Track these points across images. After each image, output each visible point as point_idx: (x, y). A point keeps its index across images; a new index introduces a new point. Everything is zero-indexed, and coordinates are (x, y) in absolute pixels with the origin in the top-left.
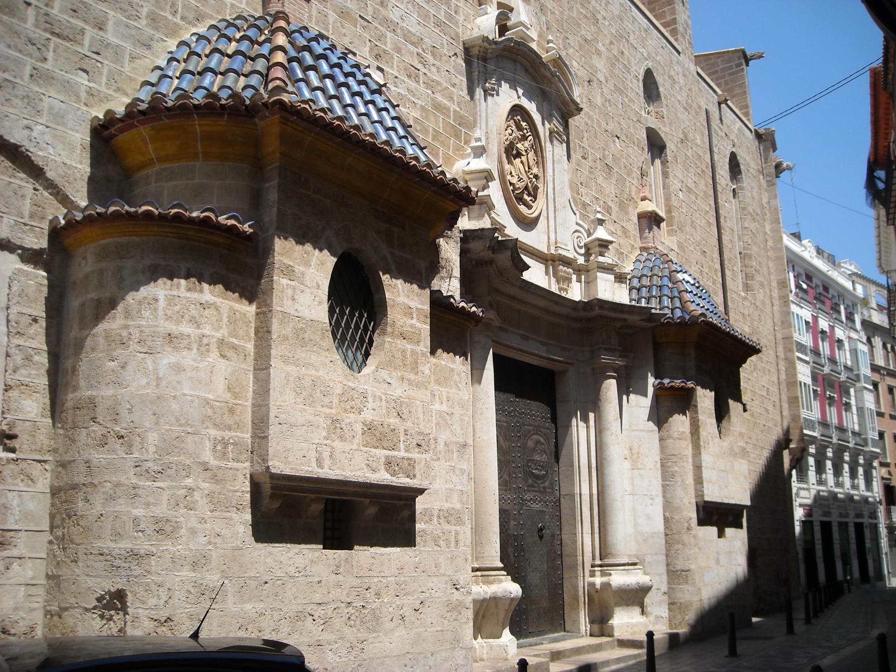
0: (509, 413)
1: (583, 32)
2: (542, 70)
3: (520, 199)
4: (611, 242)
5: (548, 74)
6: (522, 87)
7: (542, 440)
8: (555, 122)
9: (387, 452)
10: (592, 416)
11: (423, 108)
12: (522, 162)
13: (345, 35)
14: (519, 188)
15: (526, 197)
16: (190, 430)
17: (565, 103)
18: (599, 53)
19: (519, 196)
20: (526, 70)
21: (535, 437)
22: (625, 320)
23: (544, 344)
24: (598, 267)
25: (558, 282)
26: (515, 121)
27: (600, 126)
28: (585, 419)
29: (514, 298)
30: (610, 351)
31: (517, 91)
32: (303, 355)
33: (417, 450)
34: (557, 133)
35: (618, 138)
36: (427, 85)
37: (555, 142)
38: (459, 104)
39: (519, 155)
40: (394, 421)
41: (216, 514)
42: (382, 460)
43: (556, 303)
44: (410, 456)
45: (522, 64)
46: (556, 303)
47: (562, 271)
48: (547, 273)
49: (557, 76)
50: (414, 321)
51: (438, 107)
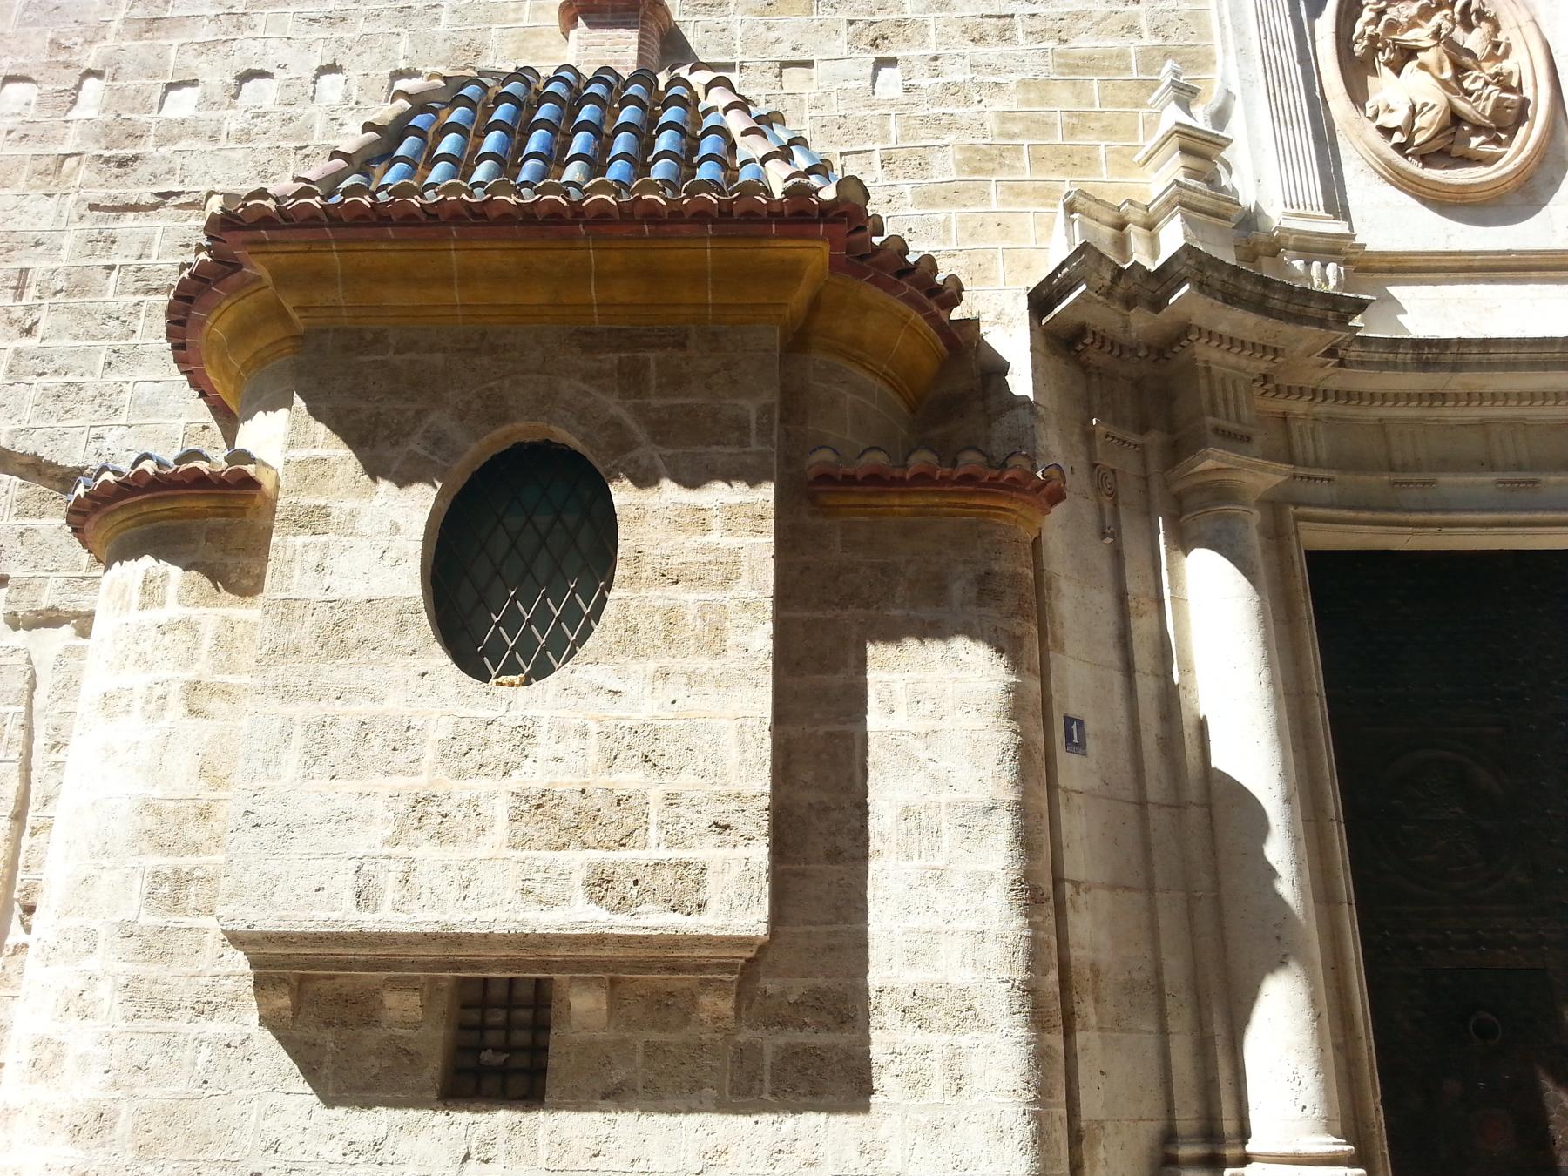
9: (597, 856)
11: (1024, 84)
12: (1423, 67)
13: (777, 41)
16: (105, 863)
19: (1439, 144)
32: (340, 675)
33: (715, 839)
36: (1039, 35)
38: (1155, 31)
40: (630, 779)
41: (141, 1025)
42: (579, 877)
44: (686, 855)
50: (713, 537)
51: (1088, 63)
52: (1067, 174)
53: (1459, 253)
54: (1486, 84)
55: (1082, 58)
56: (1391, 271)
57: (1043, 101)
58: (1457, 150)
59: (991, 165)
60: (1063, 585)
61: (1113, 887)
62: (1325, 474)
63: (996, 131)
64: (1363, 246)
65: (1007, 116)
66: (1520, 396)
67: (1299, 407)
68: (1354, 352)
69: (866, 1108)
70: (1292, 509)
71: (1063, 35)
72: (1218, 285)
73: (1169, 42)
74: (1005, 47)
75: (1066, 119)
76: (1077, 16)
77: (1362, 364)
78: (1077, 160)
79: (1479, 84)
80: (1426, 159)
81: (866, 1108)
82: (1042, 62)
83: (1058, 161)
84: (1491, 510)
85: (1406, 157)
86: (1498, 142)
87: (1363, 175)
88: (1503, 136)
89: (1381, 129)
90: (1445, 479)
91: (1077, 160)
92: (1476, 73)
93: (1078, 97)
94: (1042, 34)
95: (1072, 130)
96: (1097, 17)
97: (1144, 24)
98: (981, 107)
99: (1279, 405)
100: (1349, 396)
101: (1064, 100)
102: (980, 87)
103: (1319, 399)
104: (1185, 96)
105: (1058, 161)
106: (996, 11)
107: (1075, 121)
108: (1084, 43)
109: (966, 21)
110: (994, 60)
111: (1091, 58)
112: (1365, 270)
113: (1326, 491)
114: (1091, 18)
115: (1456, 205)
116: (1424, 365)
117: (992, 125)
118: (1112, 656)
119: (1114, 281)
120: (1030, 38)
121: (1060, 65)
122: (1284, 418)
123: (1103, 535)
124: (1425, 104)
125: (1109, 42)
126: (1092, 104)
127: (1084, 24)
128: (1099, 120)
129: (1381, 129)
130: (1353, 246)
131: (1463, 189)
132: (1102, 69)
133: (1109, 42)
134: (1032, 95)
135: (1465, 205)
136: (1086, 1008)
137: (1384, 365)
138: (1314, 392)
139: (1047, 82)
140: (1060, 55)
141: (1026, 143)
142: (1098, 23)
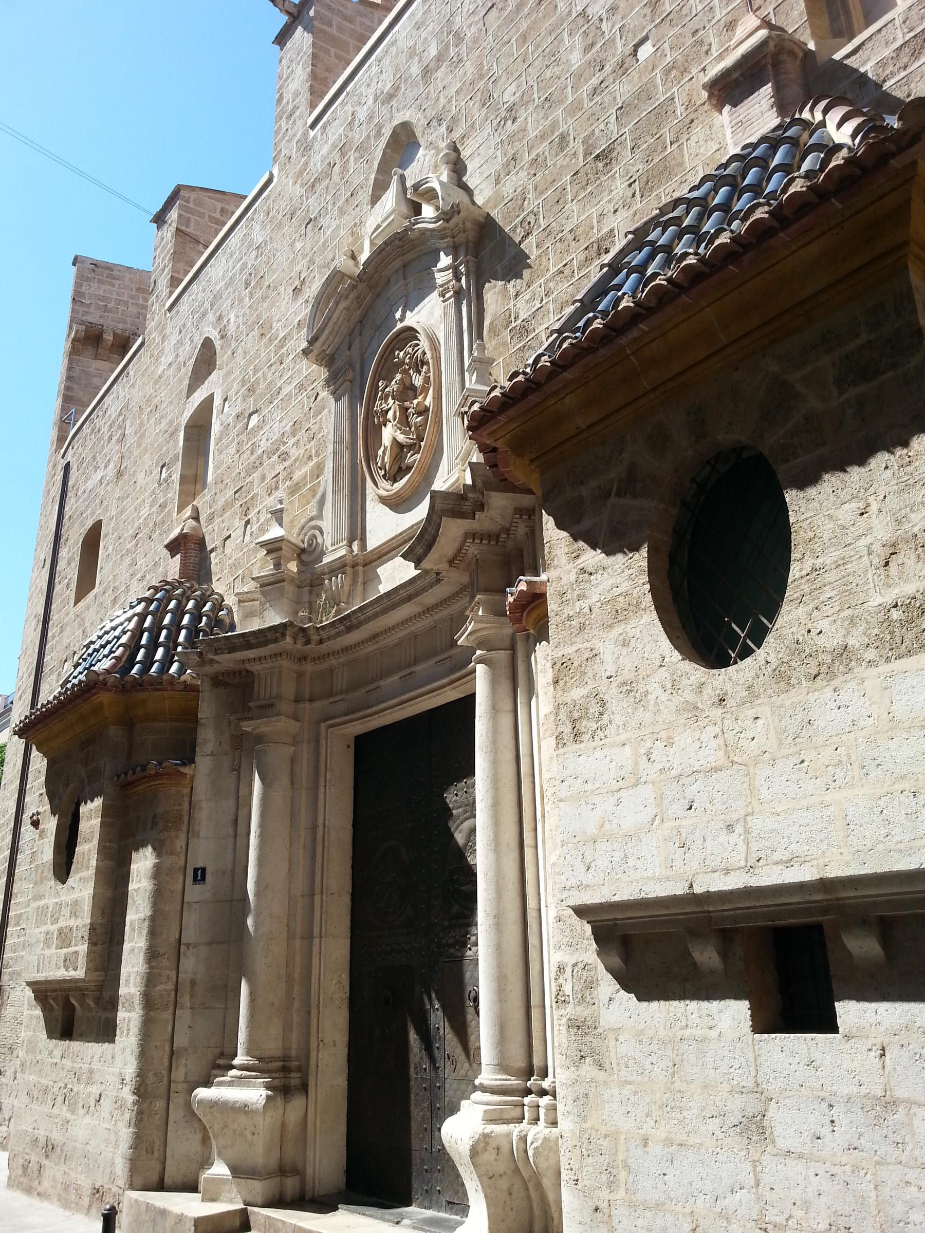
56: (379, 558)
58: (404, 467)
60: (204, 805)
61: (210, 944)
62: (341, 697)
67: (333, 662)
68: (324, 634)
69: (113, 1041)
70: (323, 724)
72: (224, 647)
77: (329, 639)
81: (113, 1041)
84: (394, 697)
90: (382, 683)
99: (324, 665)
104: (278, 515)
113: (342, 706)
115: (400, 504)
116: (349, 629)
118: (230, 831)
119: (200, 657)
122: (331, 670)
123: (234, 770)
136: (185, 1000)
137: (338, 635)
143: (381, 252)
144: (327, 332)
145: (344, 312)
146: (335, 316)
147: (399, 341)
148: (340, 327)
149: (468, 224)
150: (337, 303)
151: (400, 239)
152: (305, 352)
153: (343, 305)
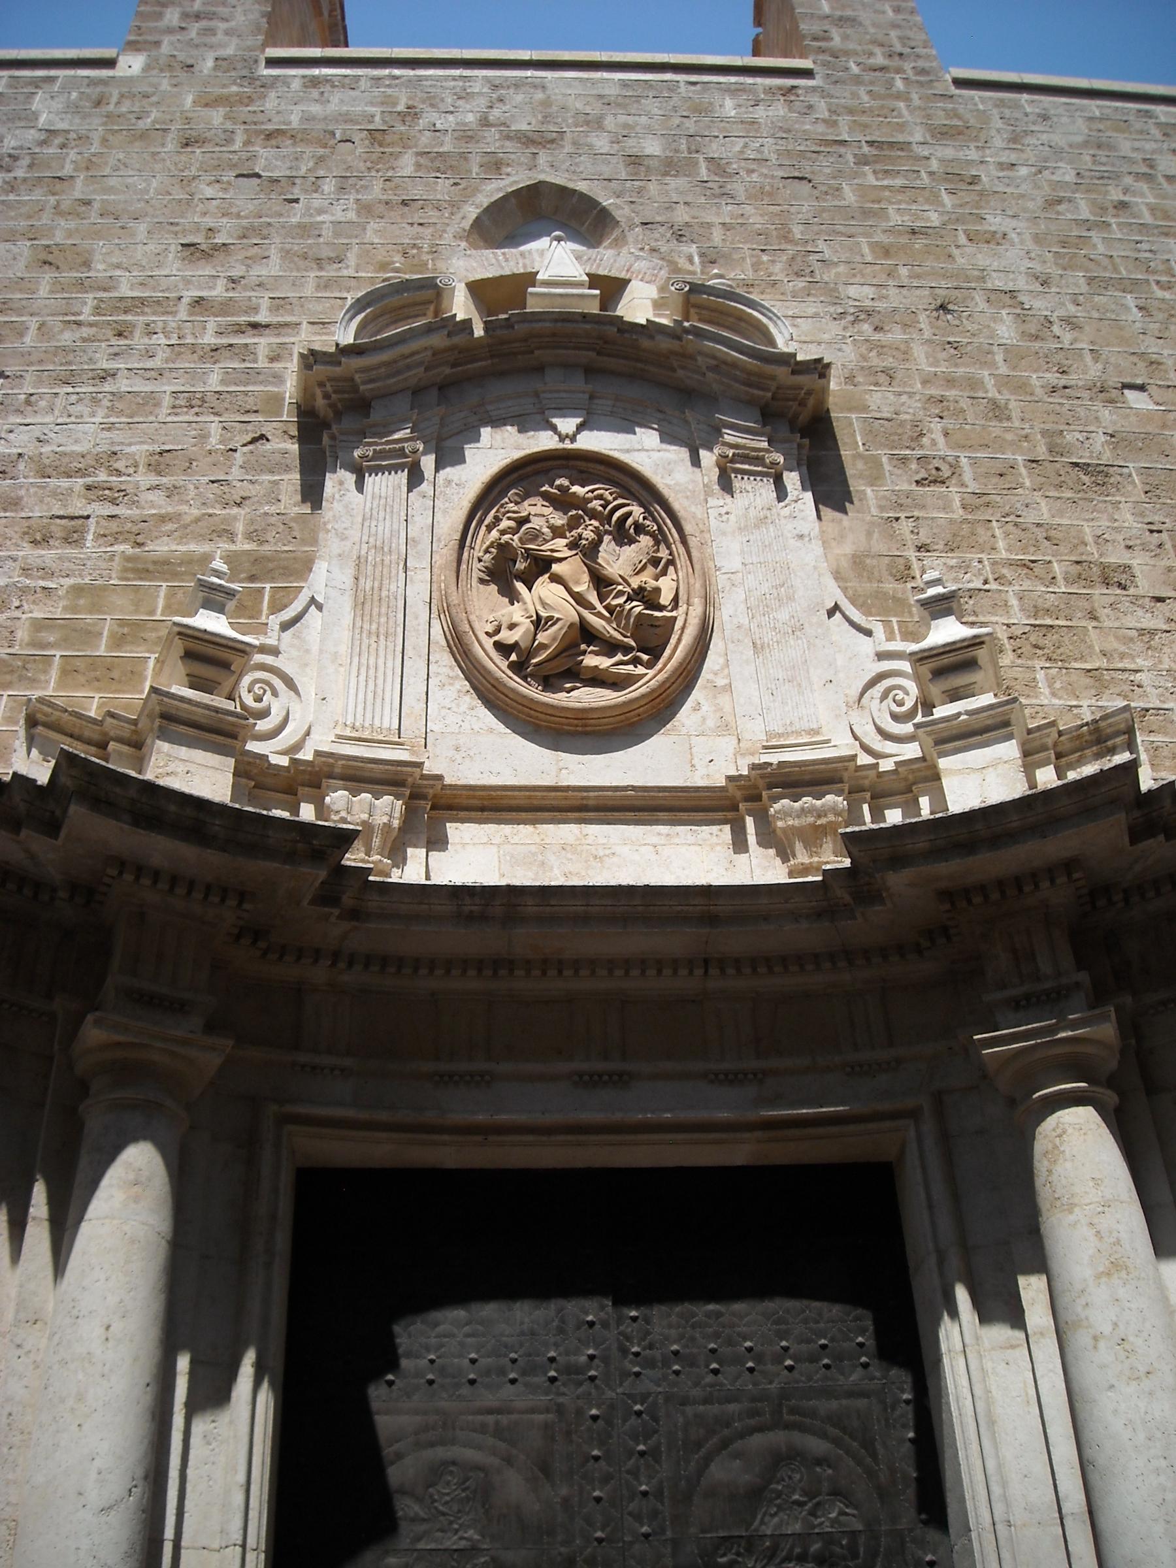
0: (571, 1370)
1: (895, 219)
2: (646, 343)
3: (563, 670)
4: (976, 642)
5: (665, 344)
6: (565, 410)
7: (816, 1445)
8: (730, 436)
10: (1032, 1288)
11: (78, 590)
12: (556, 579)
14: (543, 647)
15: (593, 660)
17: (753, 380)
18: (995, 239)
19: (563, 664)
20: (590, 371)
21: (757, 1441)
22: (1069, 865)
23: (732, 1078)
24: (938, 742)
25: (784, 854)
26: (546, 496)
27: (1022, 387)
28: (1001, 1307)
29: (500, 964)
30: (1045, 1000)
31: (554, 428)
34: (746, 459)
35: (1142, 388)
37: (737, 483)
38: (249, 536)
39: (541, 565)
43: (712, 920)
45: (567, 366)
46: (712, 920)
47: (786, 814)
48: (739, 844)
49: (687, 331)
51: (164, 568)
52: (99, 690)
53: (568, 788)
54: (630, 599)
55: (155, 563)
56: (482, 809)
57: (94, 608)
59: (8, 677)
63: (27, 639)
64: (440, 778)
65: (39, 625)
66: (611, 964)
71: (140, 539)
73: (266, 547)
74: (70, 551)
75: (116, 628)
76: (163, 518)
78: (115, 674)
79: (621, 600)
80: (549, 682)
82: (104, 565)
83: (93, 674)
85: (524, 678)
86: (636, 661)
87: (467, 698)
88: (645, 657)
89: (499, 646)
91: (115, 674)
92: (620, 587)
93: (137, 605)
94: (117, 538)
95: (118, 641)
96: (187, 519)
97: (240, 528)
98: (17, 614)
100: (384, 961)
101: (122, 608)
102: (24, 591)
103: (342, 965)
105: (93, 674)
106: (71, 511)
107: (126, 630)
108: (161, 547)
109: (32, 521)
110: (49, 563)
111: (167, 562)
112: (450, 808)
114: (178, 521)
115: (573, 734)
117: (22, 634)
120: (101, 541)
121: (126, 570)
124: (550, 618)
125: (192, 547)
126: (153, 612)
127: (170, 526)
128: (156, 630)
129: (499, 646)
130: (423, 777)
131: (582, 715)
132: (175, 575)
133: (192, 547)
134: (82, 602)
135: (586, 734)
138: (336, 956)
139: (104, 588)
140: (129, 559)
141: (58, 654)
142: (185, 527)
143: (564, 320)
144: (385, 356)
145: (429, 353)
146: (414, 345)
147: (567, 467)
148: (409, 367)
149: (811, 402)
150: (429, 329)
151: (619, 330)
152: (312, 359)
153: (437, 340)
